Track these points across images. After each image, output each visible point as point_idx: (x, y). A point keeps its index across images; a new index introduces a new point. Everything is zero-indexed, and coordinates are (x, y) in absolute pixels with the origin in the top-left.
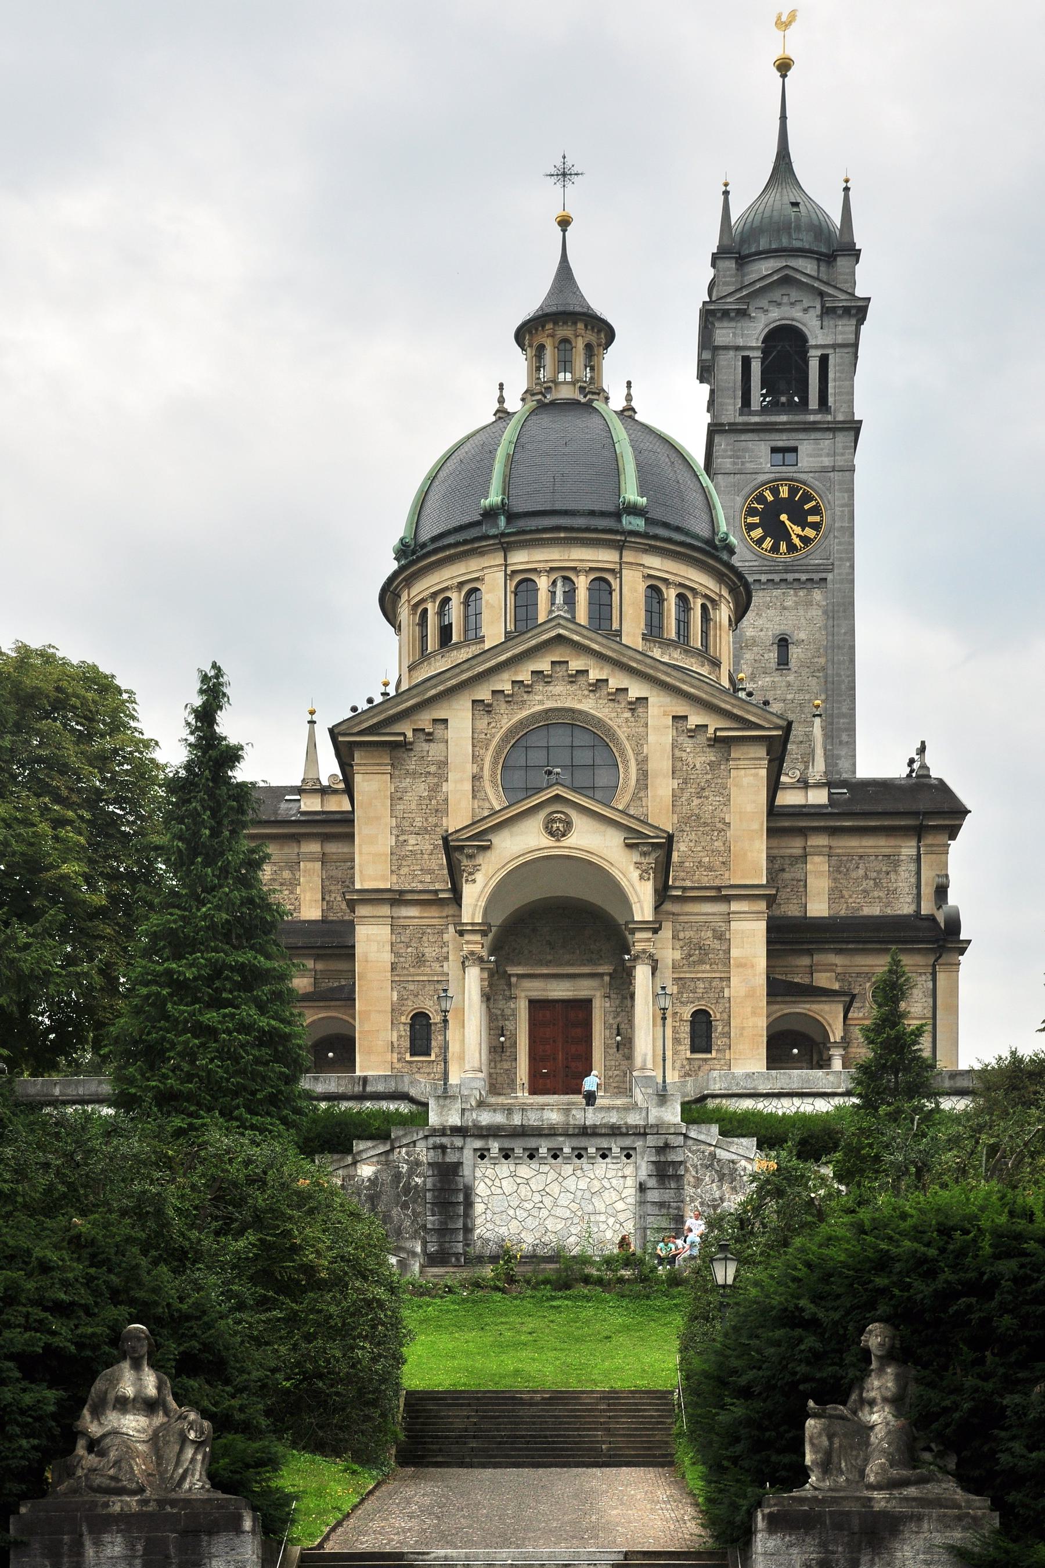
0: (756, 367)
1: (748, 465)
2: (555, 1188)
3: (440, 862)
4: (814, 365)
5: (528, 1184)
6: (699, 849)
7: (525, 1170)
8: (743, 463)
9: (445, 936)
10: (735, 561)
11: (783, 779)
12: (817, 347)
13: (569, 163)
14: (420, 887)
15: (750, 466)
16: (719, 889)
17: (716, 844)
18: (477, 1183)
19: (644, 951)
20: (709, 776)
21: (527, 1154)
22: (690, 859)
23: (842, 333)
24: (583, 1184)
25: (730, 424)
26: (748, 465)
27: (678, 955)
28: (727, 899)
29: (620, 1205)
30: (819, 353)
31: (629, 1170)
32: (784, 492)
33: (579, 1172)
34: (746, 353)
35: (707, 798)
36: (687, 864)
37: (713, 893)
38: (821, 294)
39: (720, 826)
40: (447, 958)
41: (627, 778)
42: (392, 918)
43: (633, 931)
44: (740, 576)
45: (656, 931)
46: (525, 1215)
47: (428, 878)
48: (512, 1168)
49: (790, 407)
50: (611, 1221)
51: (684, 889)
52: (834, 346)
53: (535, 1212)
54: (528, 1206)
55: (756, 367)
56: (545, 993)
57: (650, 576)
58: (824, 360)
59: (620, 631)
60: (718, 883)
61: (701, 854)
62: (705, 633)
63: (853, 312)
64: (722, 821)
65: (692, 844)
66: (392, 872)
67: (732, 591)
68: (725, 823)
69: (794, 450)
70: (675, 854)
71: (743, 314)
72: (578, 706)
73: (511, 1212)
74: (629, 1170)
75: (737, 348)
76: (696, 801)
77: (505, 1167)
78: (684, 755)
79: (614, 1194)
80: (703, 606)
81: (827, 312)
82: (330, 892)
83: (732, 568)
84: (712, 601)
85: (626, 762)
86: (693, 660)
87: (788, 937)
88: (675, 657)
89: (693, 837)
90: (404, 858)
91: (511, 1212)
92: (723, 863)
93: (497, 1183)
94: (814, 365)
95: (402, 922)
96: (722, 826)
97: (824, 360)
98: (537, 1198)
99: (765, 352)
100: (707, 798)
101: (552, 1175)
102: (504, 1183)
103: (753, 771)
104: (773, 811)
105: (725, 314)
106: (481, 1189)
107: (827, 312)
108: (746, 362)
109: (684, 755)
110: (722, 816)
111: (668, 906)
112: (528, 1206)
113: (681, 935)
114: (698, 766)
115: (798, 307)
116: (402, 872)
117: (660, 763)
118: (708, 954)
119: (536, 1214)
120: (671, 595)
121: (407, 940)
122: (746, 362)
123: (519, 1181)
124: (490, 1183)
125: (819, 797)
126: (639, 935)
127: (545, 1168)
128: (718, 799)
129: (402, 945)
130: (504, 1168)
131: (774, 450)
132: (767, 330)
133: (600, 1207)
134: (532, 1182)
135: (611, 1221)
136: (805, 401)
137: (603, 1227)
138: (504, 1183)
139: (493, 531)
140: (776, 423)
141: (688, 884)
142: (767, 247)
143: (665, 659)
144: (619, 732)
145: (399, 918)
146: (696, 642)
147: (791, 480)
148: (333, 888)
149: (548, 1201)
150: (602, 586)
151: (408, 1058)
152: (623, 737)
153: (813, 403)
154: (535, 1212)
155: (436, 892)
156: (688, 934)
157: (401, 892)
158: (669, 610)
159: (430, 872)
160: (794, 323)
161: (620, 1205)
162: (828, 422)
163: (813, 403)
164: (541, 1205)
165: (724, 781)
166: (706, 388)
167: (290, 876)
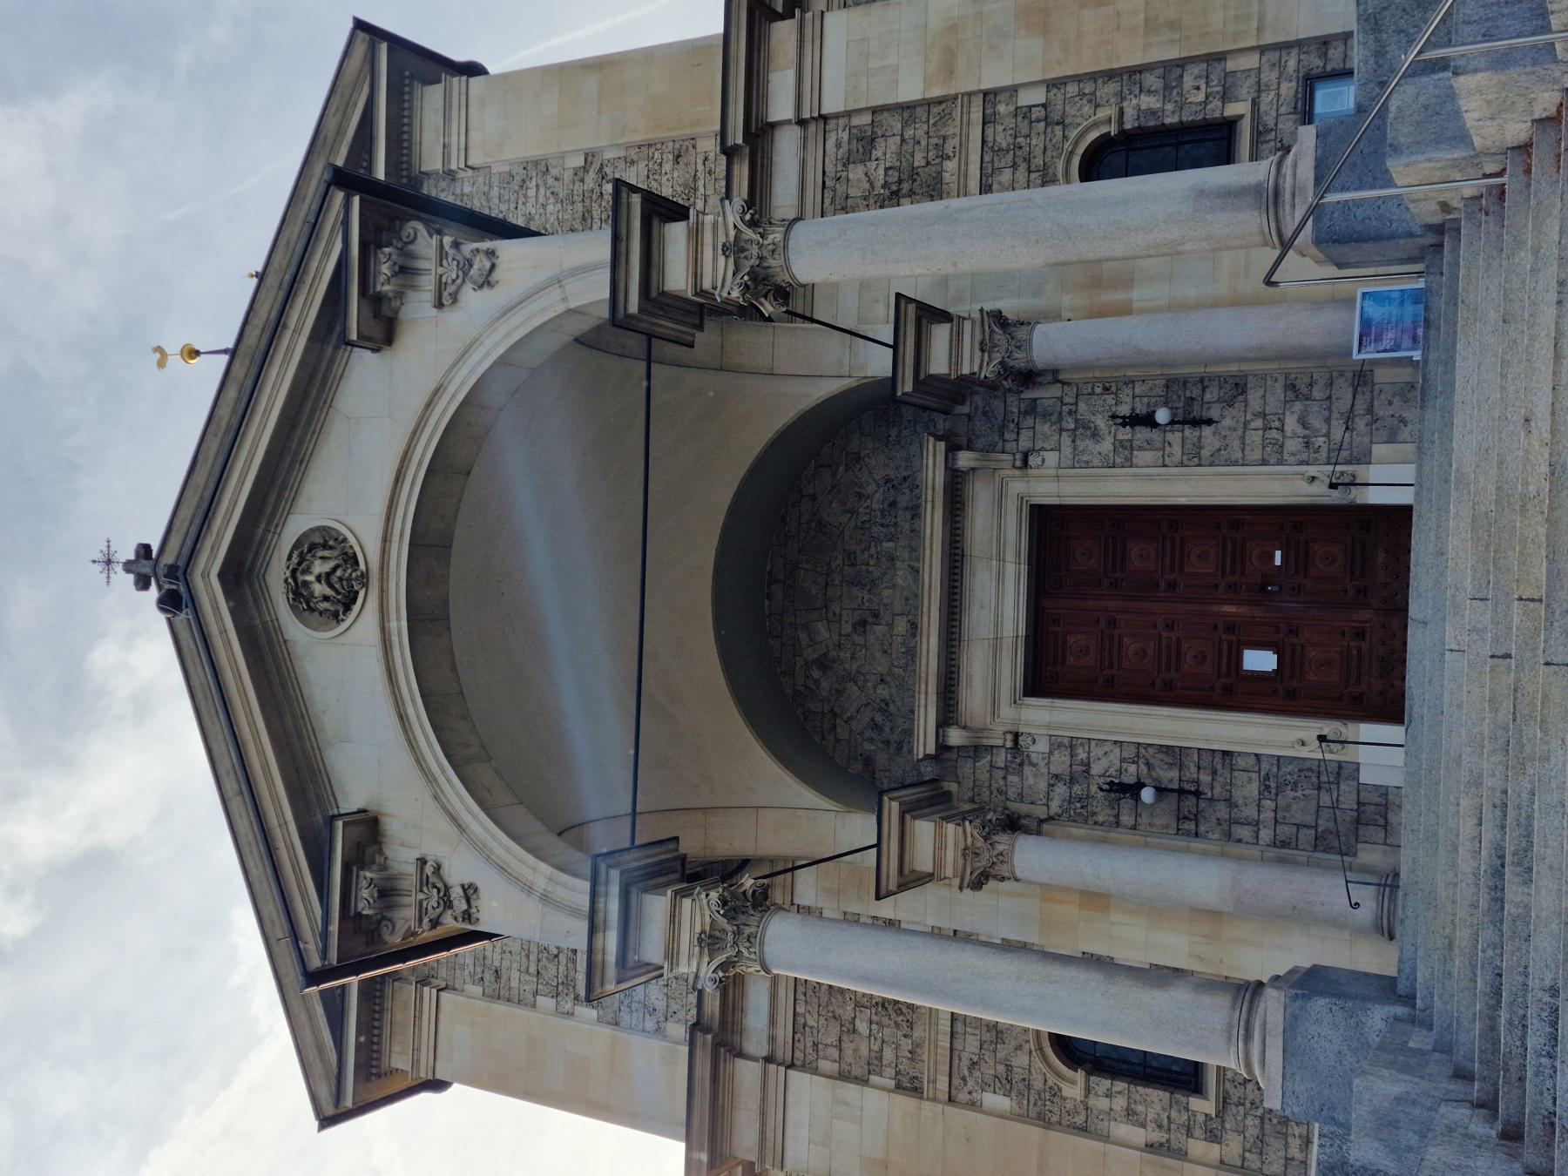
13: (99, 556)
19: (735, 249)
28: (760, 133)
37: (742, 172)
42: (769, 1059)
56: (1007, 644)
64: (580, 173)
66: (659, 1031)
68: (585, 169)
92: (677, 158)
95: (784, 1032)
96: (592, 174)
103: (473, 110)
116: (660, 1005)
121: (835, 1029)
126: (677, 278)
128: (532, 193)
129: (848, 1048)
145: (772, 1039)
157: (697, 1027)
165: (495, 181)
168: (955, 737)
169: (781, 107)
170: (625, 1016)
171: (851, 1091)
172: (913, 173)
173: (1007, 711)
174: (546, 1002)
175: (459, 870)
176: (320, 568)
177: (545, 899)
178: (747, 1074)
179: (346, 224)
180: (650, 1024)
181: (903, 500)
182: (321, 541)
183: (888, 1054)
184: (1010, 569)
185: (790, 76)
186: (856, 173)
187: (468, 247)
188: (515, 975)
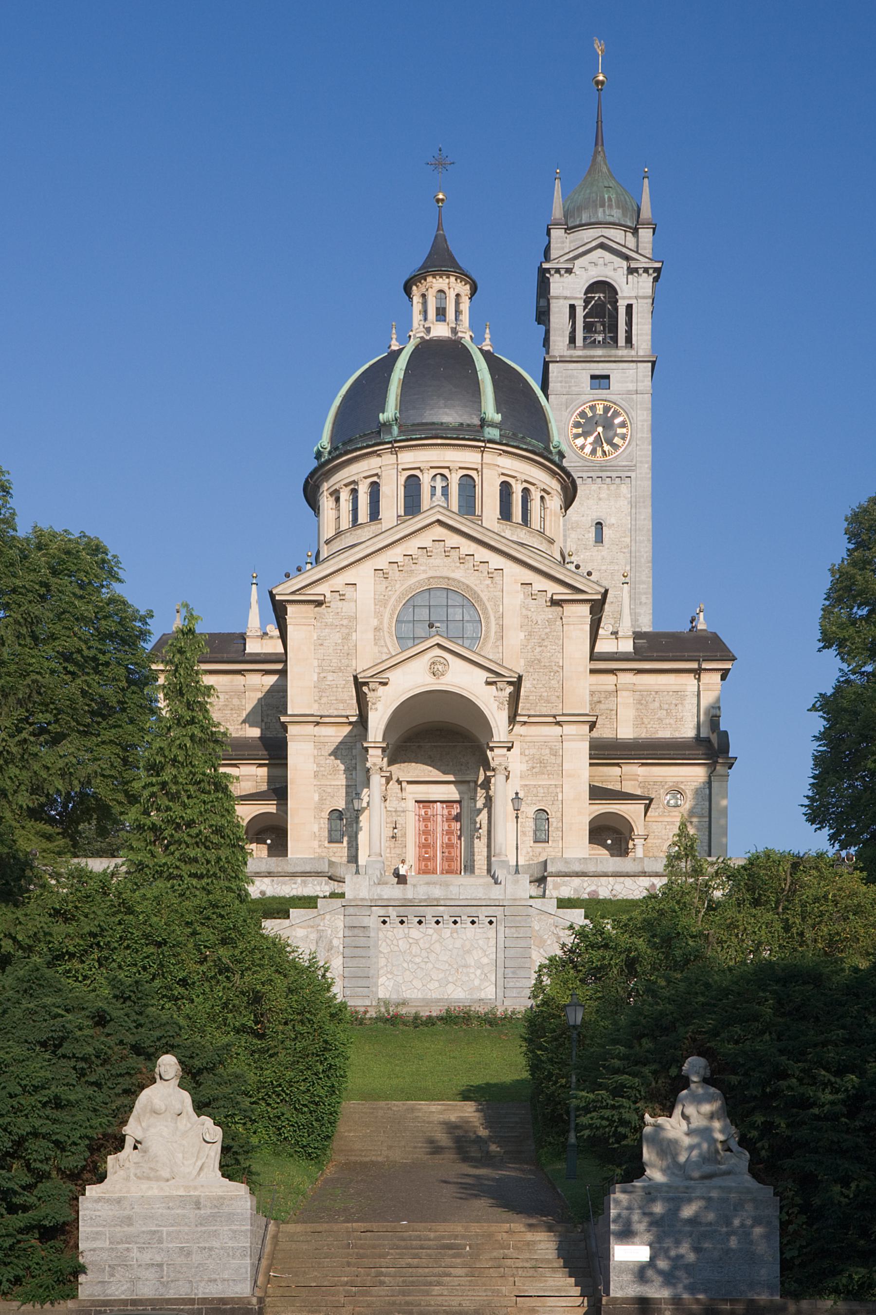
0: (580, 313)
1: (573, 388)
2: (437, 946)
3: (350, 694)
4: (622, 311)
5: (417, 943)
6: (540, 686)
7: (415, 932)
8: (570, 387)
9: (354, 751)
10: (565, 463)
11: (601, 631)
12: (624, 298)
14: (336, 713)
15: (575, 389)
16: (554, 717)
17: (552, 682)
18: (380, 942)
20: (548, 630)
21: (418, 919)
22: (534, 694)
23: (644, 288)
24: (458, 943)
25: (561, 357)
26: (573, 388)
27: (524, 767)
29: (485, 960)
30: (626, 302)
31: (492, 933)
32: (600, 410)
33: (455, 935)
34: (572, 302)
35: (546, 647)
36: (531, 698)
37: (551, 719)
38: (627, 258)
39: (555, 668)
40: (355, 768)
41: (487, 632)
43: (492, 749)
44: (568, 475)
45: (509, 749)
46: (415, 967)
47: (341, 706)
48: (406, 931)
49: (604, 344)
50: (478, 972)
51: (529, 716)
52: (636, 298)
53: (423, 965)
54: (417, 960)
55: (580, 313)
57: (503, 474)
58: (629, 307)
59: (481, 516)
60: (554, 712)
61: (542, 690)
62: (543, 519)
63: (651, 271)
65: (535, 682)
67: (564, 488)
69: (607, 377)
70: (522, 690)
71: (569, 271)
72: (452, 575)
73: (405, 965)
74: (492, 933)
75: (566, 298)
76: (538, 649)
77: (401, 931)
78: (529, 613)
79: (480, 952)
80: (542, 498)
81: (631, 271)
82: (268, 715)
83: (563, 469)
84: (548, 493)
85: (487, 618)
86: (534, 539)
87: (605, 752)
88: (522, 535)
89: (536, 676)
90: (322, 691)
91: (405, 965)
93: (395, 942)
94: (622, 311)
95: (322, 739)
97: (629, 307)
98: (424, 954)
99: (587, 301)
100: (546, 647)
101: (435, 937)
102: (401, 942)
103: (580, 626)
104: (594, 657)
105: (558, 271)
106: (384, 948)
107: (631, 271)
108: (572, 307)
109: (529, 613)
110: (557, 660)
111: (518, 729)
112: (417, 960)
113: (527, 752)
114: (539, 622)
115: (610, 267)
116: (322, 701)
117: (512, 620)
118: (547, 764)
119: (424, 967)
120: (517, 490)
122: (572, 307)
123: (411, 941)
124: (390, 943)
125: (627, 646)
126: (497, 751)
127: (430, 931)
130: (401, 930)
131: (593, 377)
132: (587, 285)
133: (470, 961)
134: (421, 942)
135: (478, 972)
136: (615, 340)
137: (472, 976)
138: (401, 942)
139: (388, 438)
140: (594, 356)
141: (533, 713)
142: (588, 221)
143: (514, 538)
144: (482, 595)
146: (535, 523)
147: (606, 401)
148: (269, 712)
149: (433, 957)
150: (468, 485)
151: (326, 844)
152: (485, 599)
153: (622, 340)
154: (423, 965)
155: (347, 717)
156: (532, 751)
158: (517, 500)
159: (343, 701)
160: (608, 280)
161: (485, 960)
162: (632, 356)
163: (622, 340)
164: (426, 960)
166: (542, 328)
167: (239, 703)
168: (404, 784)
169: (568, 729)
170: (317, 690)
171: (312, 760)
172: (545, 767)
173: (411, 796)
174: (316, 663)
175: (379, 706)
176: (440, 667)
177: (377, 728)
178: (310, 729)
179: (510, 677)
180: (316, 698)
181: (463, 767)
182: (446, 664)
183: (322, 769)
184: (446, 796)
185: (574, 733)
186: (548, 751)
187: (506, 703)
188: (322, 651)
